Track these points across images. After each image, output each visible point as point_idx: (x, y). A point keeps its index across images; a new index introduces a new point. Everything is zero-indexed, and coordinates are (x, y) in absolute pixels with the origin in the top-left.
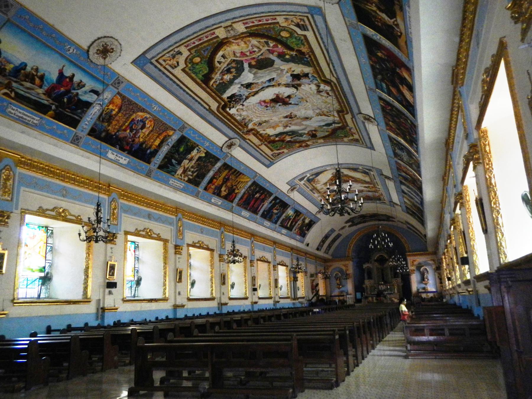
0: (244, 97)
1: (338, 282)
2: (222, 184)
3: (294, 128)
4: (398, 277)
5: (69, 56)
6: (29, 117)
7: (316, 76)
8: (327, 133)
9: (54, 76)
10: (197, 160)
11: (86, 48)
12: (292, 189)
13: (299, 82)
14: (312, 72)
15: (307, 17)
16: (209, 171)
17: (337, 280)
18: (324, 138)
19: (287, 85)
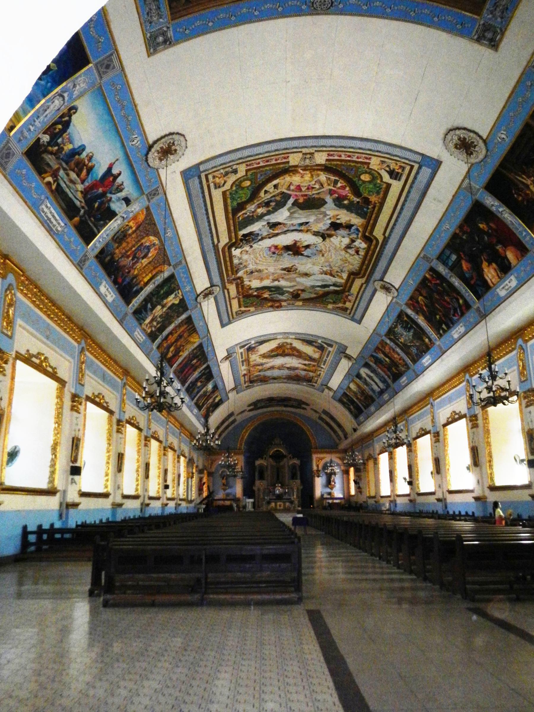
0: (260, 238)
1: (224, 481)
2: (173, 343)
3: (283, 283)
4: (296, 479)
5: (130, 149)
6: (56, 220)
7: (361, 229)
8: (313, 296)
9: (100, 171)
10: (169, 308)
11: (151, 142)
13: (333, 232)
14: (360, 224)
15: (412, 167)
16: (170, 323)
17: (223, 479)
18: (305, 300)
19: (316, 234)
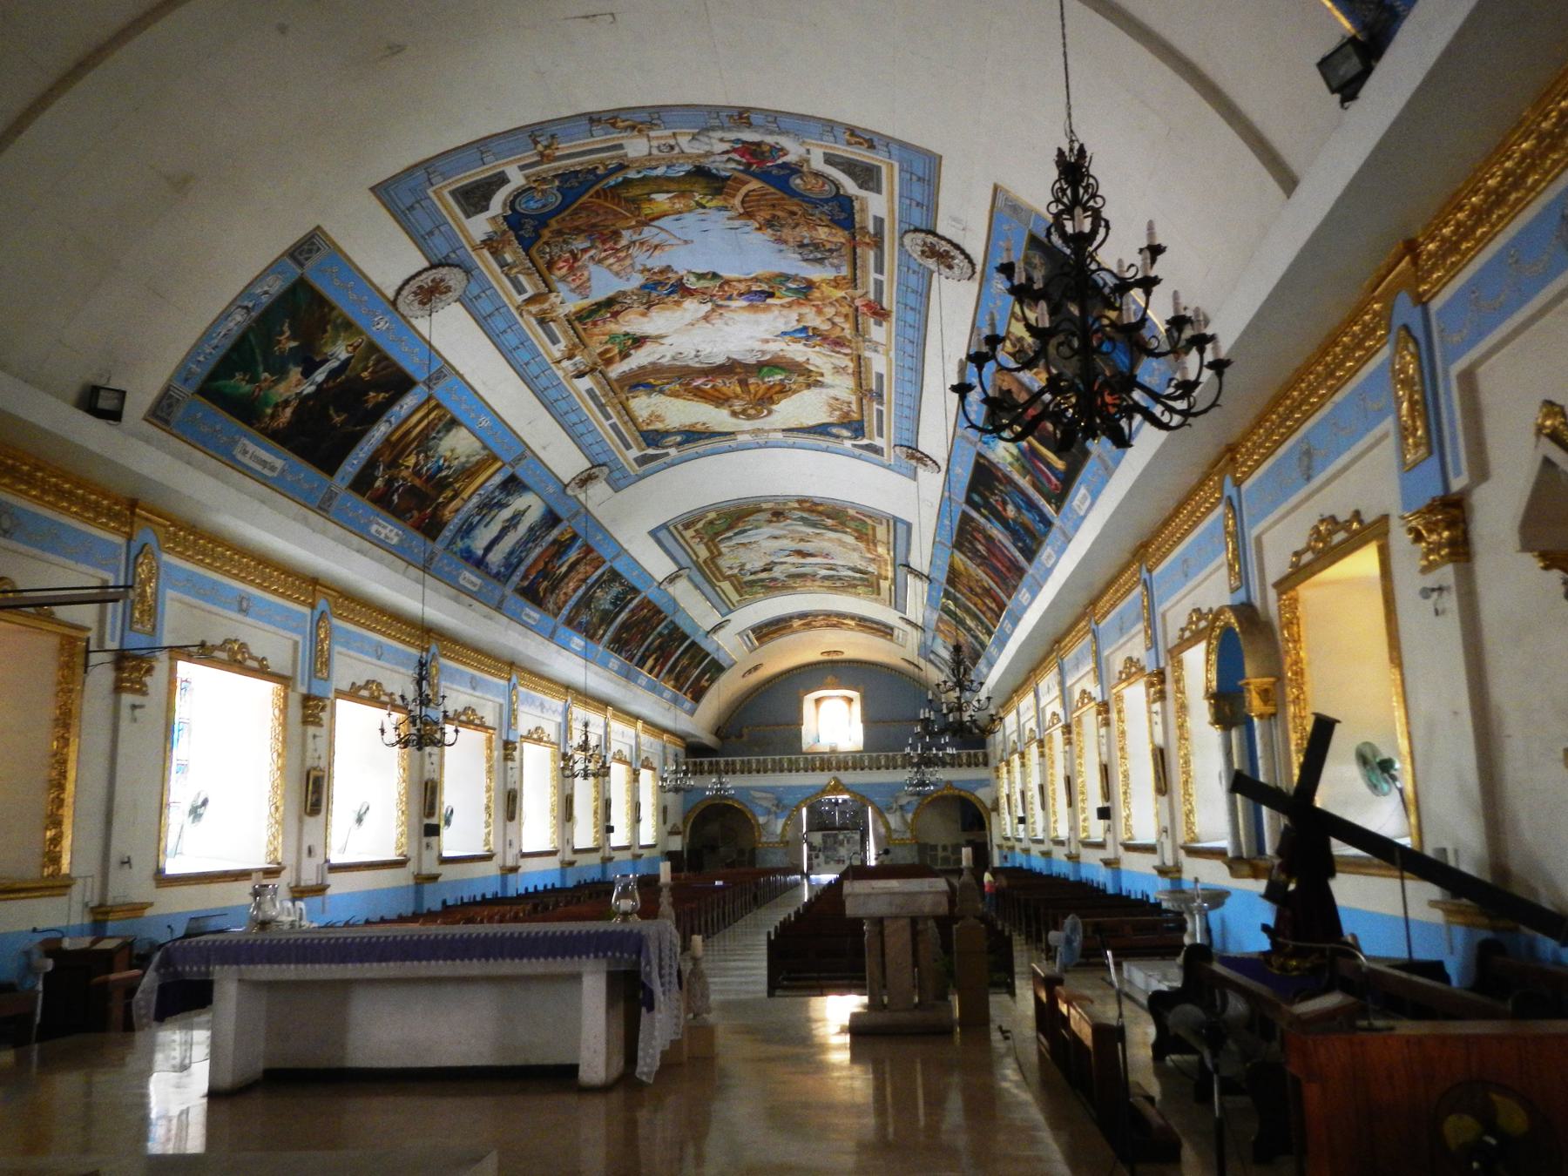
3: (810, 530)
12: (921, 458)
18: (760, 510)
